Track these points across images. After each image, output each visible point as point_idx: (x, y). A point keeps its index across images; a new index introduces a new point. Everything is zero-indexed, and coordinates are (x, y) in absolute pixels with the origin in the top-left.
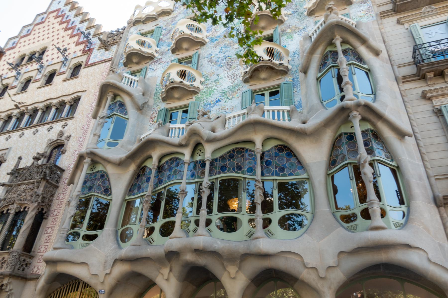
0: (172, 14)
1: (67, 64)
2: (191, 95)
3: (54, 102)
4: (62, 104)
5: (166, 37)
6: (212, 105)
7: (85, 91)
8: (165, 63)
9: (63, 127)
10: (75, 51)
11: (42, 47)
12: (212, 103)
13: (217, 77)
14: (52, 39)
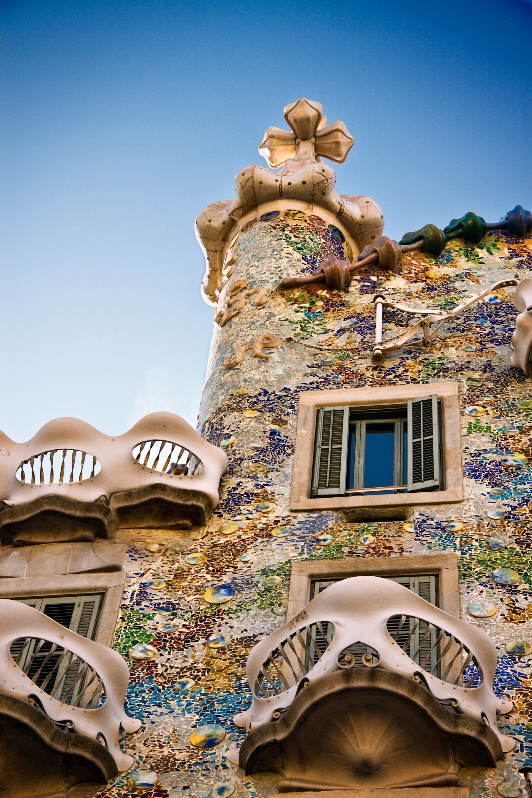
0: (213, 525)
5: (177, 660)
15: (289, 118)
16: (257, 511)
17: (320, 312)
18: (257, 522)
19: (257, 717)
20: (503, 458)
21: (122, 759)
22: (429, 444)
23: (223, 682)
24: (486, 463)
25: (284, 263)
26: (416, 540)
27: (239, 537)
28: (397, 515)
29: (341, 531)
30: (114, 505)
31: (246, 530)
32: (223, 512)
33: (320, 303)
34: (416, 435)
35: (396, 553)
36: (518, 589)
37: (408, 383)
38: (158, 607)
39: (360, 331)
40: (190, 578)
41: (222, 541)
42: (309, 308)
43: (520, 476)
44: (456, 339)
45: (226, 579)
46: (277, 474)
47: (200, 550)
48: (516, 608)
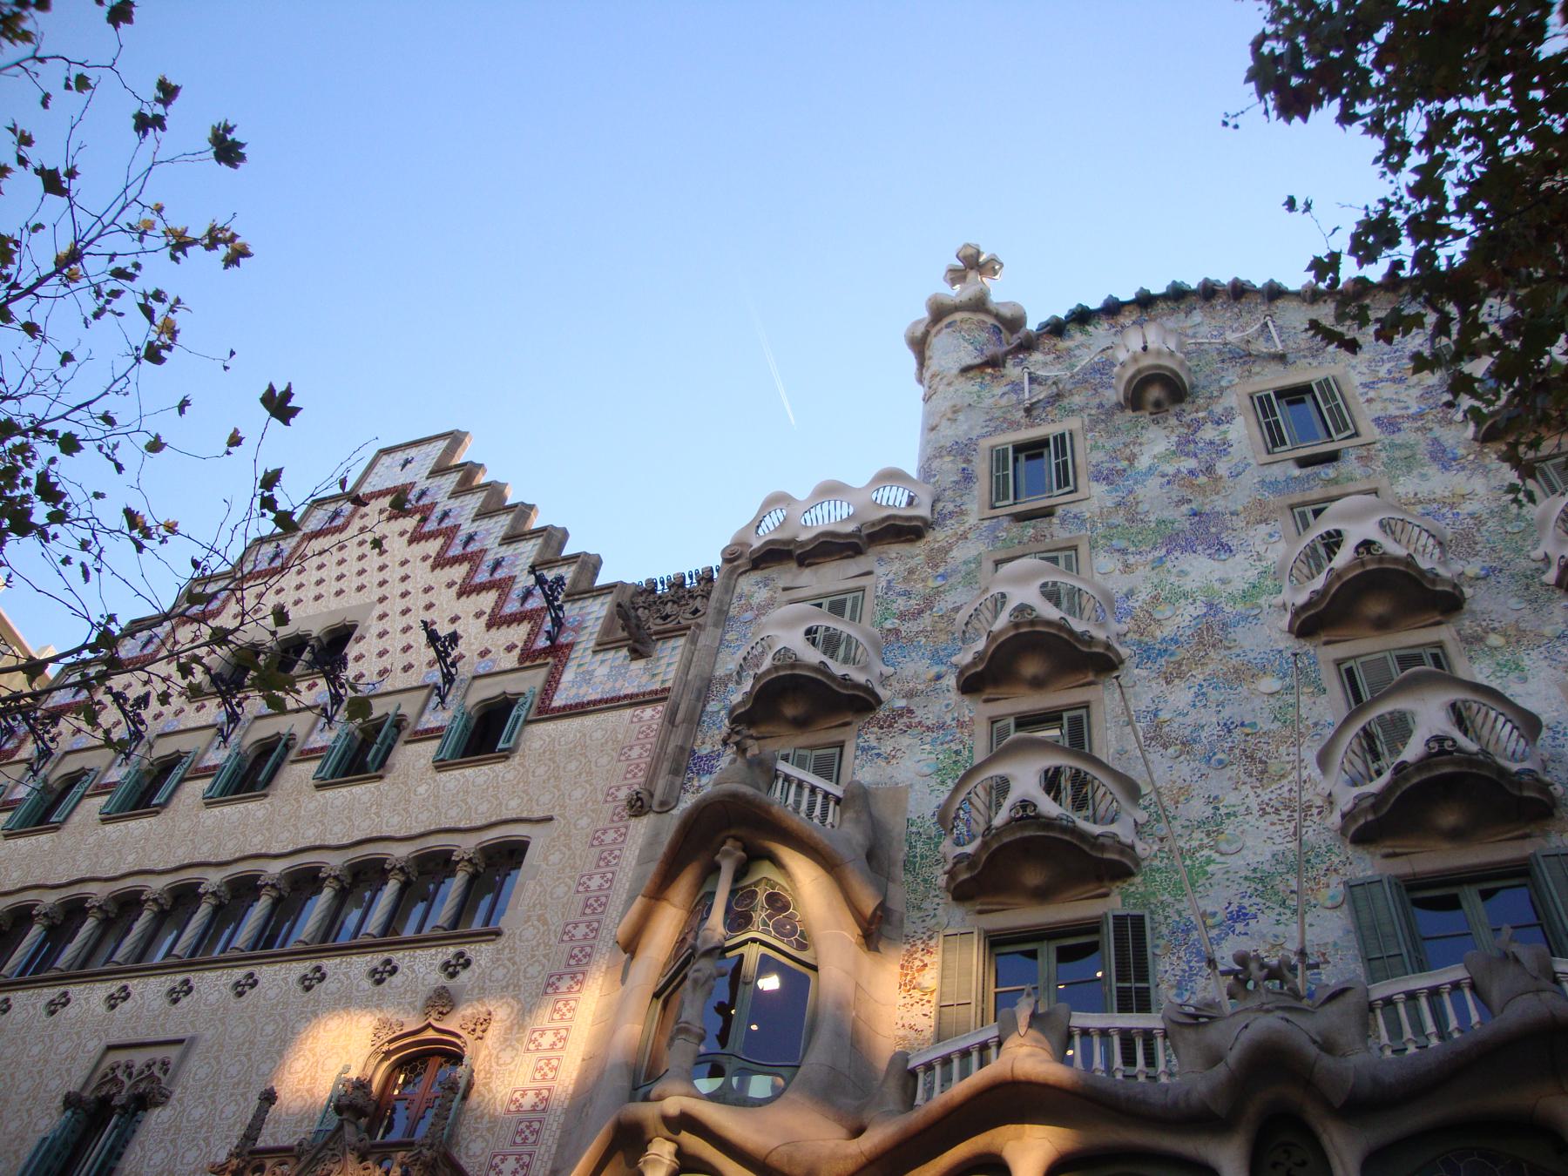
0: (930, 536)
1: (449, 698)
2: (1100, 879)
3: (401, 852)
4: (435, 865)
6: (1214, 933)
7: (550, 819)
8: (928, 728)
9: (451, 970)
10: (491, 651)
11: (335, 621)
12: (1210, 922)
13: (1209, 811)
14: (378, 593)
19: (965, 658)
21: (883, 693)
22: (1065, 463)
23: (943, 637)
28: (1047, 513)
30: (865, 532)
34: (1057, 457)
38: (899, 594)
39: (1015, 392)
45: (941, 570)
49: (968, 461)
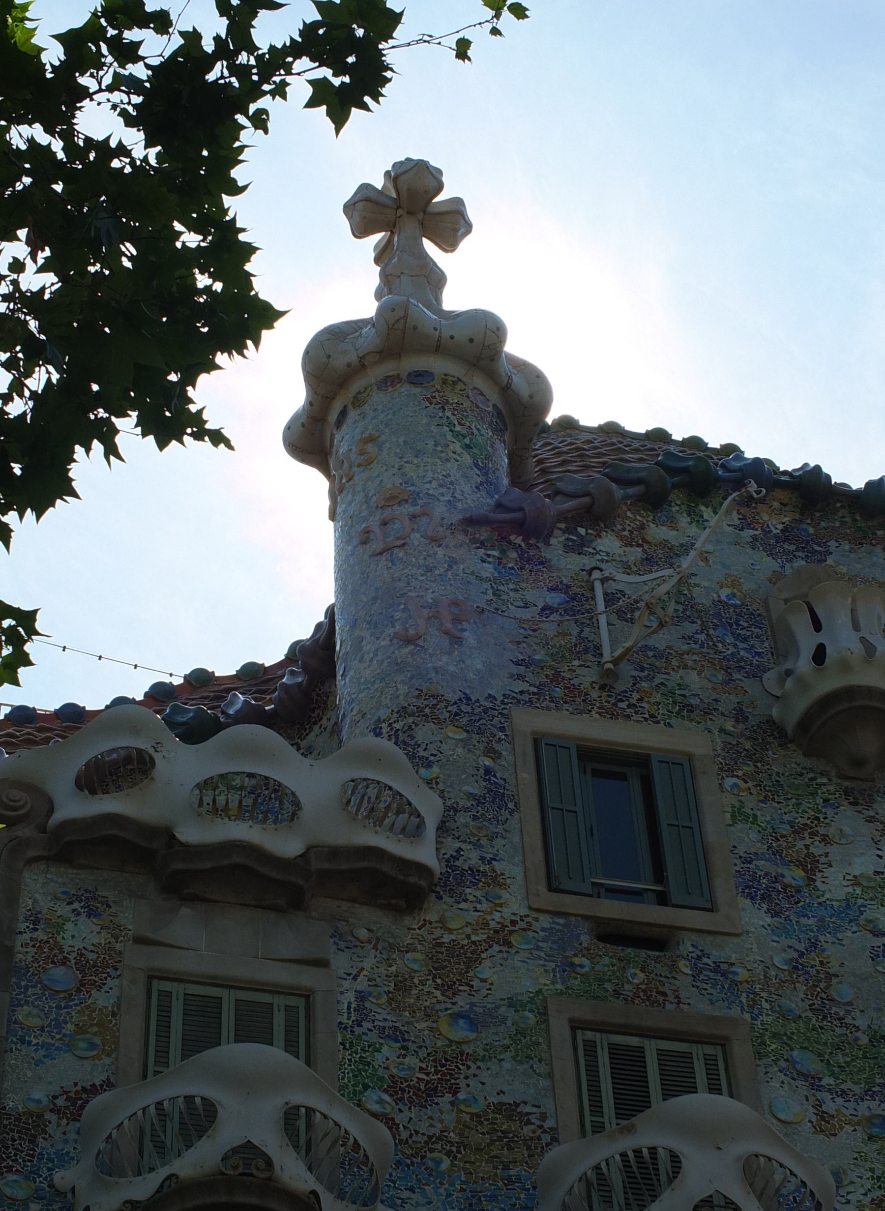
0: (432, 912)
15: (398, 182)
16: (487, 899)
17: (512, 568)
18: (489, 917)
20: (779, 871)
24: (760, 876)
25: (452, 467)
26: (693, 986)
27: (468, 937)
29: (600, 955)
31: (475, 927)
32: (442, 893)
33: (514, 555)
35: (671, 1003)
36: (822, 1083)
37: (646, 719)
40: (414, 992)
41: (446, 939)
42: (499, 558)
43: (802, 903)
44: (695, 657)
45: (462, 1002)
46: (503, 842)
47: (419, 947)
48: (823, 1112)
49: (491, 752)
